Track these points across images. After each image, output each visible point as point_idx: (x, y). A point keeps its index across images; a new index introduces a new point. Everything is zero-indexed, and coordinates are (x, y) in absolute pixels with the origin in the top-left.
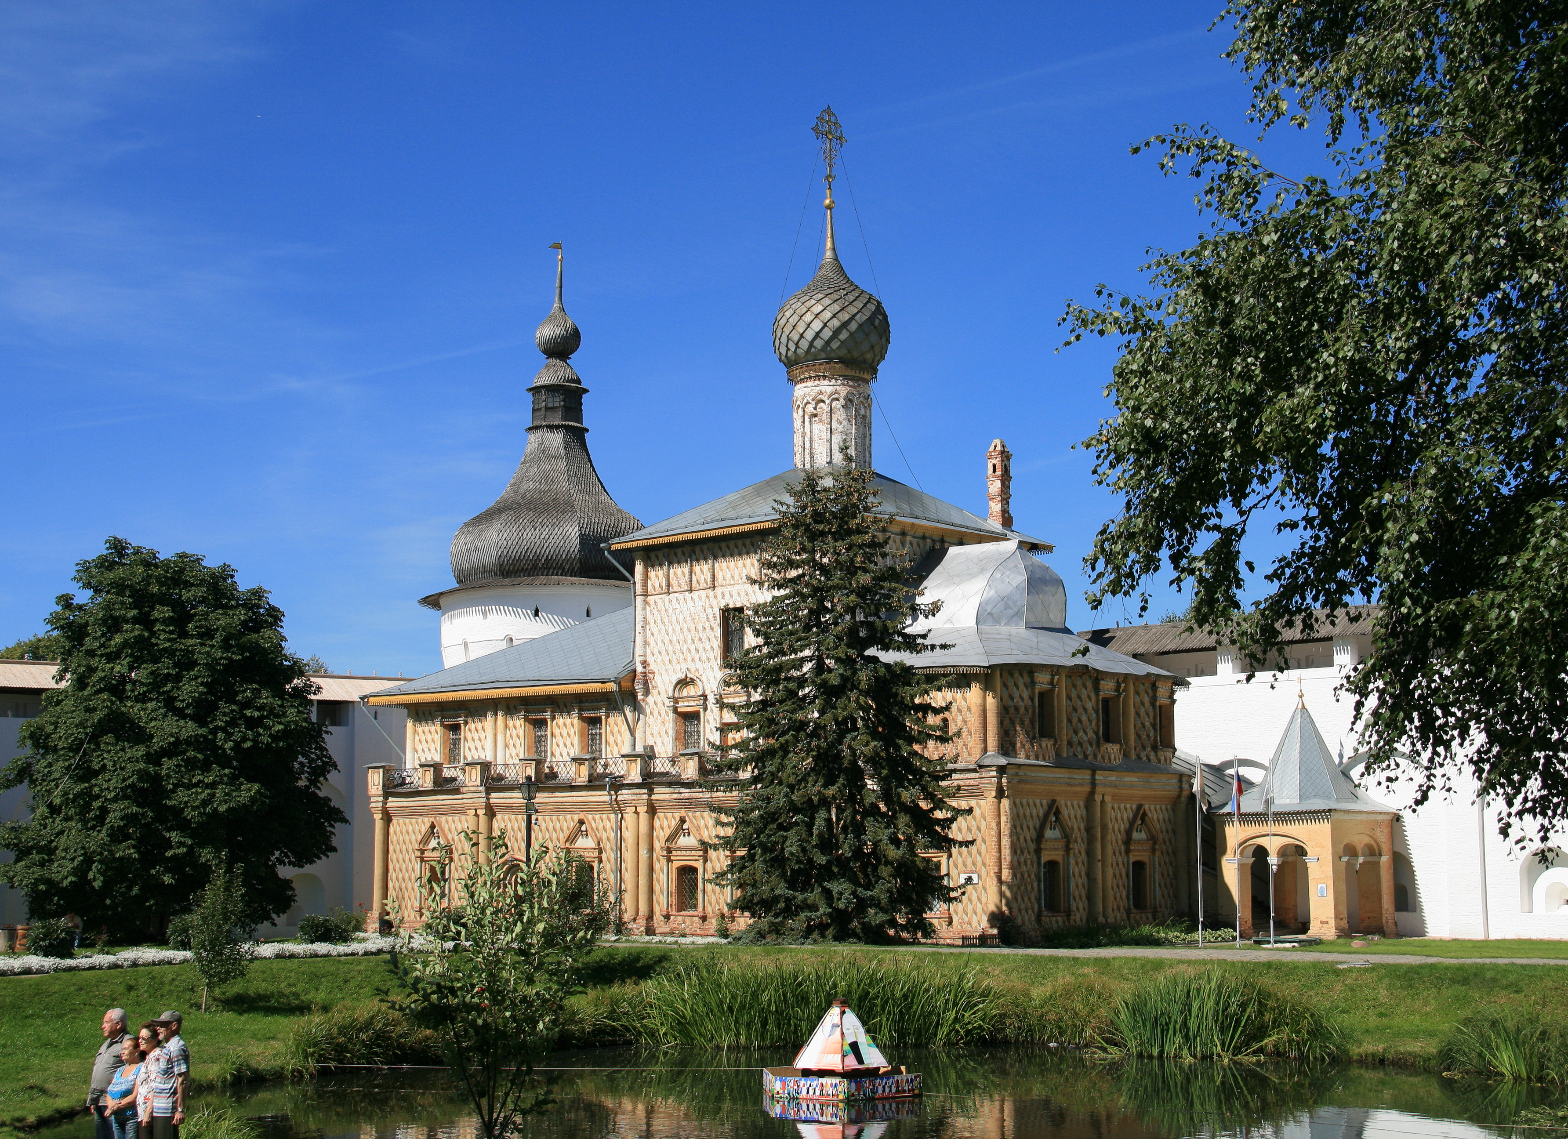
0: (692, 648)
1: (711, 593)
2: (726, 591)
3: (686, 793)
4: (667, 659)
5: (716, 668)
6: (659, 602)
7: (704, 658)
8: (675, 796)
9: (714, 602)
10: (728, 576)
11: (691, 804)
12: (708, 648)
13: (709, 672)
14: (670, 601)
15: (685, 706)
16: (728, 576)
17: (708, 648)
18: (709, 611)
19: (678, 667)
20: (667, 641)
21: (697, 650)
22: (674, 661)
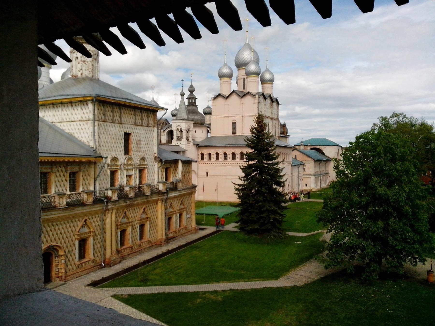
0: (115, 146)
1: (121, 126)
2: (126, 126)
3: (128, 202)
4: (106, 149)
5: (123, 154)
6: (102, 125)
7: (119, 150)
8: (125, 204)
9: (122, 130)
10: (125, 121)
11: (130, 206)
12: (120, 146)
13: (120, 155)
14: (106, 125)
15: (114, 168)
16: (125, 121)
17: (120, 146)
18: (120, 132)
19: (109, 153)
20: (105, 141)
21: (116, 147)
22: (108, 150)
